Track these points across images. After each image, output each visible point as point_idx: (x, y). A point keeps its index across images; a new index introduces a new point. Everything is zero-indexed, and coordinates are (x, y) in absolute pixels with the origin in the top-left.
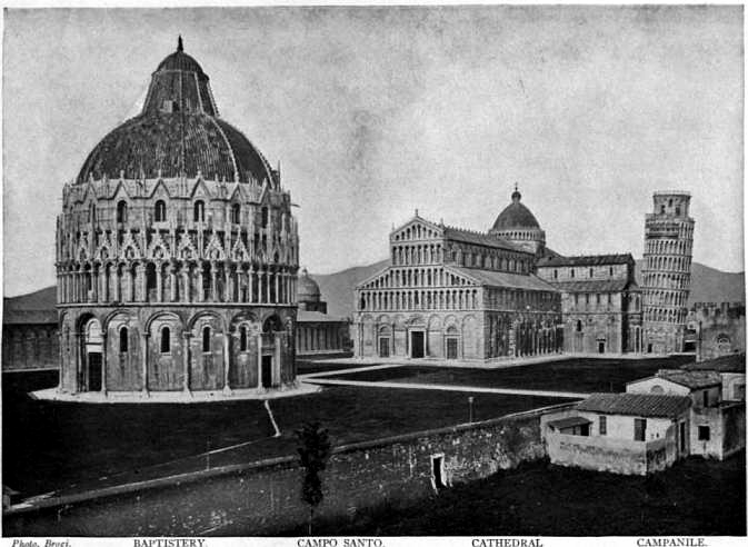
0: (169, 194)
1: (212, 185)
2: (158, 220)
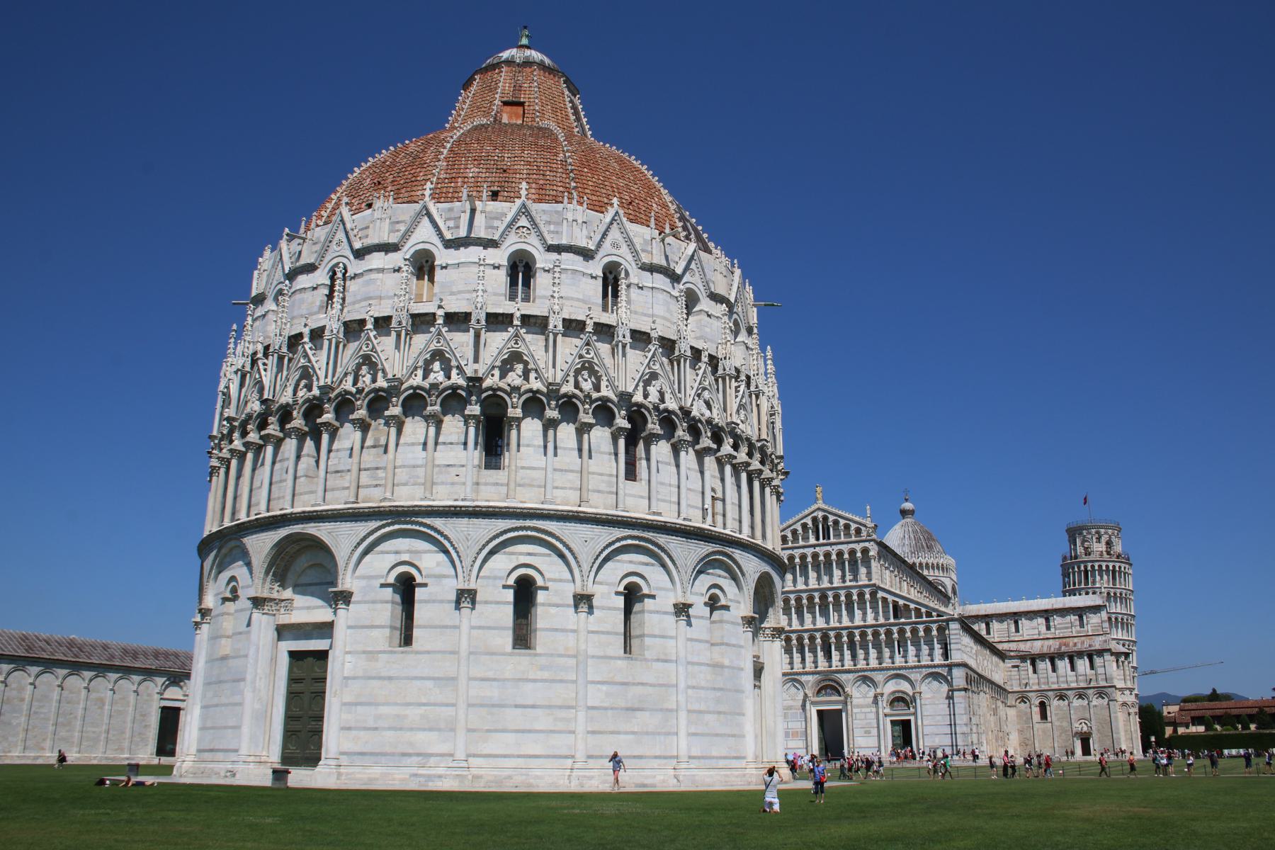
0: (543, 239)
1: (641, 233)
2: (512, 297)
